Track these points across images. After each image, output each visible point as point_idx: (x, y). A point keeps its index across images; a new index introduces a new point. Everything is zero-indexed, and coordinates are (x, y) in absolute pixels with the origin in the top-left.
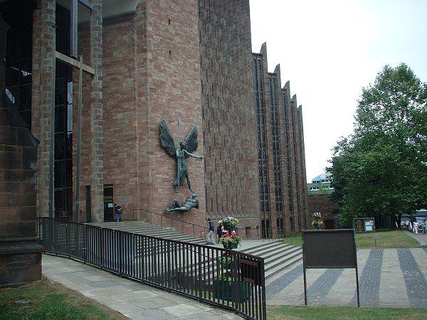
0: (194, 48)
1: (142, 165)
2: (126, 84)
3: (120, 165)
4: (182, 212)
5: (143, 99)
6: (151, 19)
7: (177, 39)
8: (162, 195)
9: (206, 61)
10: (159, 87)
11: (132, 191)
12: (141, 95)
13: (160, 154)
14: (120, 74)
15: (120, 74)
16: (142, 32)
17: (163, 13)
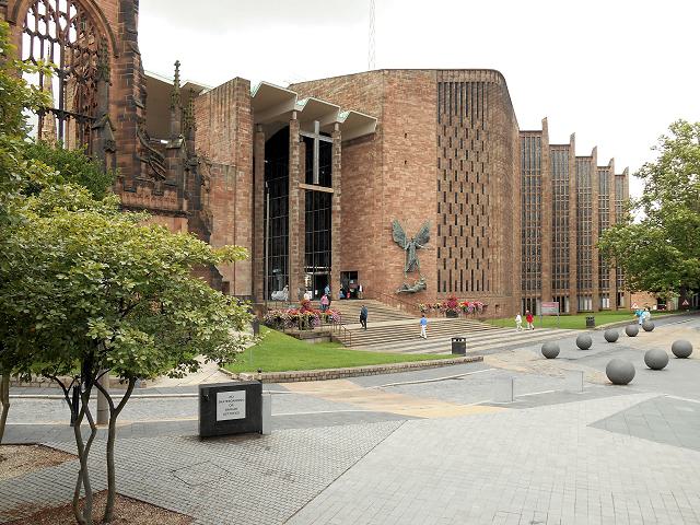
0: (434, 152)
1: (378, 256)
2: (368, 192)
3: (362, 256)
4: (413, 293)
5: (380, 204)
6: (387, 137)
7: (414, 149)
8: (395, 279)
9: (445, 162)
10: (394, 192)
11: (370, 276)
12: (378, 201)
13: (392, 248)
14: (363, 184)
15: (363, 184)
16: (381, 149)
17: (400, 130)
